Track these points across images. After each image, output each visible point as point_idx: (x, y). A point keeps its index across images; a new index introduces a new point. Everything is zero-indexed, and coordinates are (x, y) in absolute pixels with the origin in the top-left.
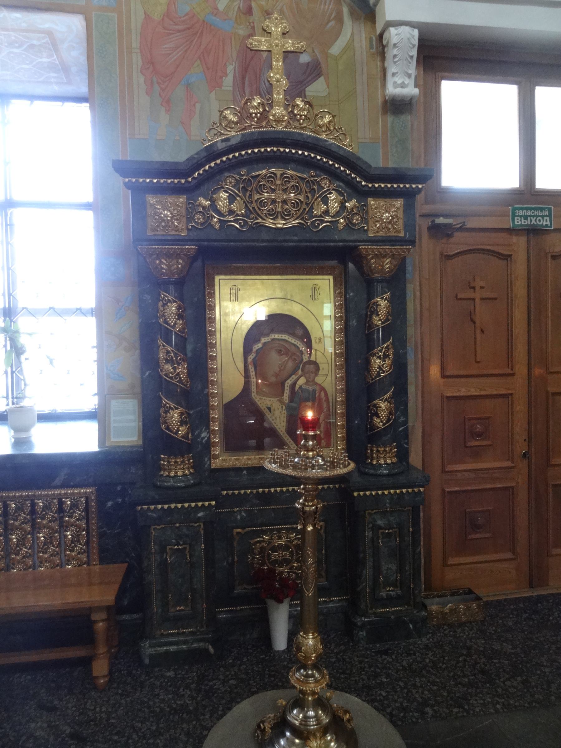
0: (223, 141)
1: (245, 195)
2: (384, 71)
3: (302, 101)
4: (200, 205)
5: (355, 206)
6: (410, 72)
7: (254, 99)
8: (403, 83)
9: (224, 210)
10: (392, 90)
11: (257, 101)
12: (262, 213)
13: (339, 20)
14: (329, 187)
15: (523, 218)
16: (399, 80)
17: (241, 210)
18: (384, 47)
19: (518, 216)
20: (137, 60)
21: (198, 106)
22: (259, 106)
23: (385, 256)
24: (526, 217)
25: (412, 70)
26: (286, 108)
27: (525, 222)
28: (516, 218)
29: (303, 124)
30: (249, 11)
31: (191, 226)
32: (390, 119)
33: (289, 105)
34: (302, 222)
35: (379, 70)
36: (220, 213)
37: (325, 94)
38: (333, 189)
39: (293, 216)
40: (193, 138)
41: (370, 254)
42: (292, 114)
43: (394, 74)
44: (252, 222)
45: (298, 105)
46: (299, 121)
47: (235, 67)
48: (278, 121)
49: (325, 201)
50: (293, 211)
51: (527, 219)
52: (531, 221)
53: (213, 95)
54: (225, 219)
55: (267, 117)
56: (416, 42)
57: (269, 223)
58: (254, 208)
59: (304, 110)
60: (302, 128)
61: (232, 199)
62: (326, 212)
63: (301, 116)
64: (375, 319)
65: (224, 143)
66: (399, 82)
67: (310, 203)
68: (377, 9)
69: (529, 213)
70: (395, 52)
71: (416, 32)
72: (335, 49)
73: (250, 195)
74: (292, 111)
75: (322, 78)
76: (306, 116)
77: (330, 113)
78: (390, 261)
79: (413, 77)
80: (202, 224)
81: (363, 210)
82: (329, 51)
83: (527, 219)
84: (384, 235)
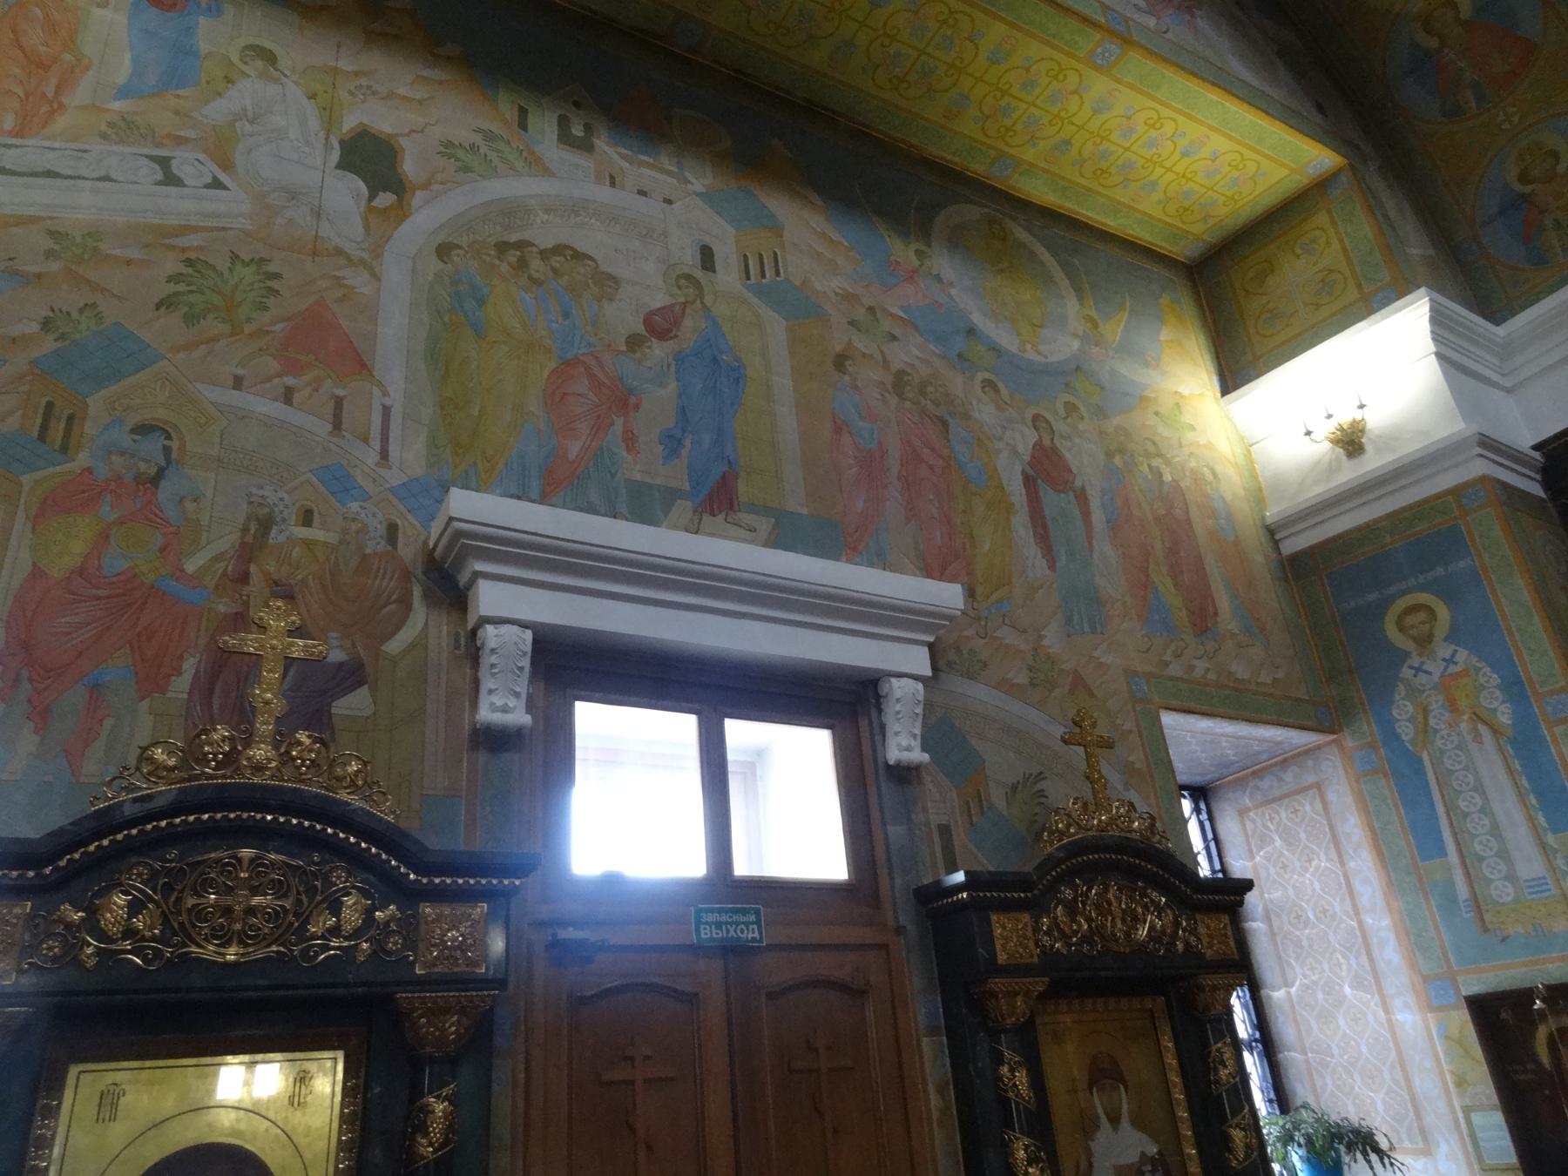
0: (135, 800)
1: (166, 897)
3: (309, 737)
4: (60, 920)
5: (392, 918)
6: (518, 689)
7: (215, 730)
9: (114, 930)
10: (485, 715)
11: (222, 731)
12: (200, 934)
13: (406, 604)
14: (345, 882)
15: (713, 927)
16: (499, 701)
17: (151, 928)
18: (478, 649)
19: (707, 923)
22: (223, 741)
23: (447, 1011)
24: (719, 925)
25: (522, 687)
26: (276, 747)
27: (717, 934)
28: (702, 927)
29: (305, 774)
30: (244, 578)
31: (28, 963)
32: (482, 757)
33: (282, 738)
34: (282, 949)
35: (468, 680)
36: (102, 936)
37: (368, 712)
38: (354, 887)
39: (264, 938)
40: (83, 780)
41: (416, 1009)
42: (286, 759)
43: (490, 692)
44: (171, 953)
45: (299, 743)
46: (298, 768)
47: (200, 662)
48: (259, 768)
49: (335, 908)
50: (267, 928)
51: (721, 930)
52: (728, 931)
53: (145, 705)
54: (114, 947)
55: (237, 760)
56: (528, 647)
57: (209, 951)
58: (181, 924)
59: (311, 751)
60: (303, 781)
61: (135, 907)
62: (335, 931)
63: (303, 761)
64: (419, 1143)
65: (138, 805)
66: (499, 703)
67: (302, 915)
68: (470, 593)
69: (724, 918)
70: (493, 659)
72: (394, 646)
73: (178, 900)
74: (288, 752)
75: (364, 691)
77: (359, 758)
78: (458, 1021)
79: (524, 696)
80: (55, 959)
81: (410, 927)
82: (383, 648)
83: (721, 930)
84: (446, 970)
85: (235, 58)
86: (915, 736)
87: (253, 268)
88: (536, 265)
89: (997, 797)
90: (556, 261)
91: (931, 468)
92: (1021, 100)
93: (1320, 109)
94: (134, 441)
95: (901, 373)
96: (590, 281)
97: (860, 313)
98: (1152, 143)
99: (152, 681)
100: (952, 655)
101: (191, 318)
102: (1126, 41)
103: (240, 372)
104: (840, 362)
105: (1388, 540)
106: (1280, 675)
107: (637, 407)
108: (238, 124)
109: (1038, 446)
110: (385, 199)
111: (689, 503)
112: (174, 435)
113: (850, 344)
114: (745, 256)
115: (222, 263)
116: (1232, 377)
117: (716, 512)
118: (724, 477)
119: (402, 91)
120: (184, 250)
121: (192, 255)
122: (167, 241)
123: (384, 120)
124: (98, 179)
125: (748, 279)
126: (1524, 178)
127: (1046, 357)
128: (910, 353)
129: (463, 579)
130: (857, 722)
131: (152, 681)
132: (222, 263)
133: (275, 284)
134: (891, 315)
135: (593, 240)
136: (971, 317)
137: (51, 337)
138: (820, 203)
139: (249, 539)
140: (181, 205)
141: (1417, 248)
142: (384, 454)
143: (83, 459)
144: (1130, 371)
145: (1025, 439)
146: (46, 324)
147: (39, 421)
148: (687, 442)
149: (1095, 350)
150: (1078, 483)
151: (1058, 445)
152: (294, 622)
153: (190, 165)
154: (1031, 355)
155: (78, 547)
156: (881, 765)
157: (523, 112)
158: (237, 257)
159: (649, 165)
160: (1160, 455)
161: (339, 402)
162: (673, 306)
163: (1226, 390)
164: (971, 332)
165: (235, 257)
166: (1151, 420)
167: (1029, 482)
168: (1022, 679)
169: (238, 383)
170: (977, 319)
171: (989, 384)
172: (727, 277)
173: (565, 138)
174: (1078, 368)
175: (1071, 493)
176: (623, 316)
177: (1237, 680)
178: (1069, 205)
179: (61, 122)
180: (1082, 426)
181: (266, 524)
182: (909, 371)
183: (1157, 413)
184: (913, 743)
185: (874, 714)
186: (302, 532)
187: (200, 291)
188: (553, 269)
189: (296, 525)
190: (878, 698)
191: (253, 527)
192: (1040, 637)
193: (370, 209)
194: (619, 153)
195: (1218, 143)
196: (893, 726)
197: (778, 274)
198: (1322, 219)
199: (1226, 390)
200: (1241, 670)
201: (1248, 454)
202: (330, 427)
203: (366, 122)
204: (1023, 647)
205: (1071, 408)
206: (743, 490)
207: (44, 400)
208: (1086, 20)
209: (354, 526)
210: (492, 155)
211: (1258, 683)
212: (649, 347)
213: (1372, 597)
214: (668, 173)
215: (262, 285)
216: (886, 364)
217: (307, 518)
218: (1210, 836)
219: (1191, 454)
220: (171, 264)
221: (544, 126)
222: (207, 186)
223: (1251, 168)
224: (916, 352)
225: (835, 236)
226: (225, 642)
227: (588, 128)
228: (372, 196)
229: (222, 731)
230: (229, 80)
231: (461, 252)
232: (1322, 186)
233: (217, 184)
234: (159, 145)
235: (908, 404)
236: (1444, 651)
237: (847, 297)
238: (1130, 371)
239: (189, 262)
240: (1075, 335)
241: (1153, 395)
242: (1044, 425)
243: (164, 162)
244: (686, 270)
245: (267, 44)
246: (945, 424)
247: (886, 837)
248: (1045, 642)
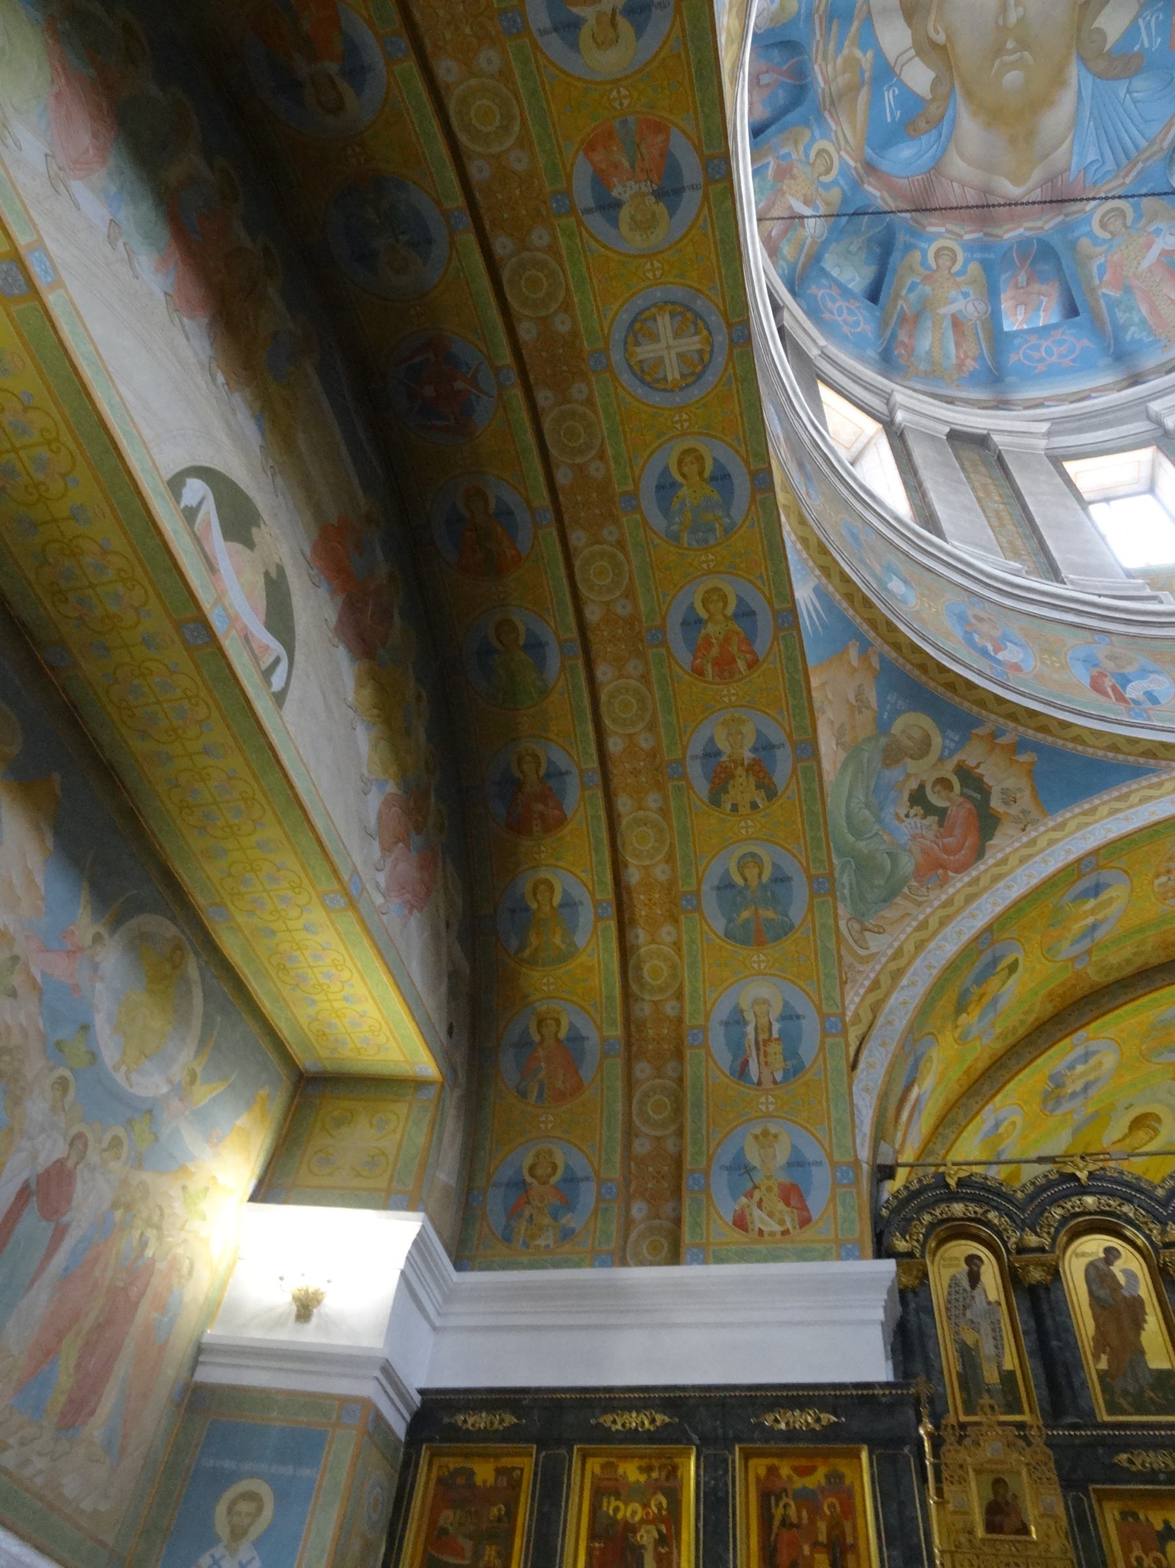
92: (262, 883)
98: (329, 976)
102: (352, 904)
105: (274, 1414)
109: (60, 1164)
126: (532, 1169)
127: (131, 1086)
138: (50, 843)
141: (446, 1174)
144: (190, 1137)
145: (52, 1149)
149: (175, 1103)
150: (65, 1219)
151: (78, 1172)
154: (120, 1078)
160: (159, 1228)
163: (253, 1198)
164: (86, 1028)
166: (175, 1192)
170: (100, 1022)
171: (63, 1084)
174: (150, 1111)
175: (53, 1225)
180: (113, 1165)
183: (184, 1188)
195: (369, 1007)
198: (402, 1108)
199: (253, 1198)
200: (70, 1487)
205: (116, 1143)
208: (335, 871)
213: (228, 1464)
219: (185, 1241)
223: (382, 1039)
225: (39, 879)
232: (419, 1084)
236: (245, 1551)
238: (190, 1137)
240: (170, 1081)
241: (193, 1169)
242: (81, 1146)
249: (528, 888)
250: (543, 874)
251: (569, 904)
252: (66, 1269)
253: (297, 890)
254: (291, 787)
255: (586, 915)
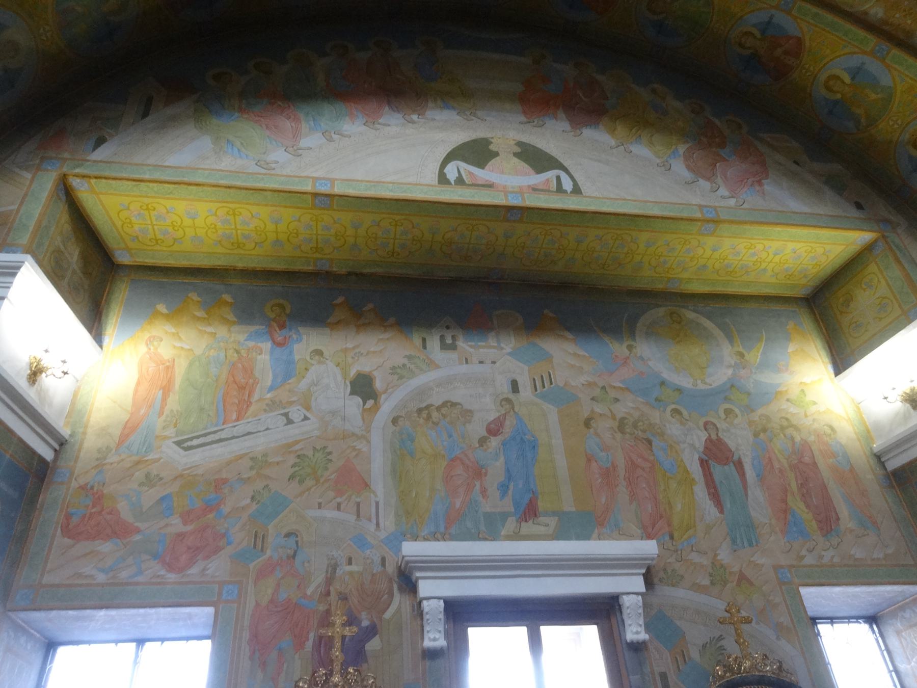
2: (422, 626)
6: (440, 629)
8: (435, 637)
10: (427, 643)
13: (391, 595)
16: (432, 636)
20: (246, 635)
21: (285, 665)
22: (323, 675)
30: (328, 594)
32: (428, 663)
45: (350, 673)
53: (297, 656)
59: (354, 675)
66: (432, 637)
71: (442, 603)
72: (388, 615)
75: (378, 636)
76: (355, 680)
85: (308, 358)
86: (641, 626)
87: (321, 451)
88: (435, 415)
89: (695, 654)
90: (444, 410)
91: (643, 469)
93: (859, 206)
94: (286, 541)
95: (622, 419)
96: (460, 416)
97: (597, 392)
98: (754, 254)
99: (299, 645)
100: (662, 574)
101: (301, 482)
102: (716, 222)
103: (320, 500)
104: (587, 423)
106: (890, 551)
107: (486, 474)
108: (311, 389)
109: (709, 440)
110: (370, 403)
111: (514, 518)
112: (299, 536)
113: (592, 411)
114: (534, 379)
115: (310, 453)
116: (841, 363)
117: (528, 520)
118: (531, 501)
119: (372, 349)
120: (296, 451)
121: (299, 453)
122: (290, 450)
123: (364, 365)
124: (264, 431)
125: (536, 390)
127: (711, 385)
128: (627, 406)
129: (414, 580)
130: (610, 620)
131: (299, 645)
132: (310, 453)
133: (329, 457)
134: (614, 387)
135: (459, 394)
136: (662, 375)
137: (254, 503)
138: (571, 336)
139: (329, 575)
140: (293, 432)
142: (378, 524)
143: (269, 553)
144: (767, 378)
145: (699, 438)
146: (253, 498)
147: (253, 540)
148: (511, 487)
149: (742, 372)
150: (736, 458)
151: (721, 437)
152: (344, 620)
153: (296, 413)
154: (701, 386)
155: (270, 591)
156: (624, 642)
157: (424, 340)
158: (315, 448)
159: (483, 347)
161: (358, 504)
162: (499, 417)
163: (838, 371)
164: (663, 383)
165: (314, 448)
166: (784, 406)
167: (704, 463)
168: (706, 582)
169: (320, 506)
170: (666, 375)
171: (676, 411)
172: (526, 392)
173: (444, 347)
174: (732, 386)
175: (732, 464)
176: (477, 429)
177: (856, 560)
178: (719, 289)
179: (252, 409)
181: (334, 567)
182: (628, 417)
183: (788, 400)
184: (639, 629)
185: (618, 614)
186: (348, 568)
187: (303, 468)
188: (442, 414)
189: (346, 565)
190: (620, 606)
191: (330, 569)
192: (716, 555)
193: (364, 410)
194: (469, 346)
195: (791, 246)
196: (628, 622)
197: (551, 383)
198: (873, 268)
199: (838, 371)
200: (858, 553)
201: (858, 410)
202: (355, 517)
203: (359, 369)
204: (705, 563)
205: (728, 412)
206: (541, 505)
207: (255, 530)
208: (691, 220)
209: (368, 561)
210: (412, 367)
211: (873, 560)
212: (490, 442)
214: (494, 347)
215: (326, 459)
216: (614, 417)
217: (350, 562)
218: (883, 648)
219: (814, 420)
220: (292, 459)
221: (434, 343)
222: (303, 420)
223: (820, 250)
224: (631, 405)
225: (581, 353)
226: (321, 633)
227: (453, 337)
228: (364, 404)
229: (322, 671)
230: (307, 369)
231: (402, 419)
232: (869, 249)
233: (306, 418)
234: (284, 408)
235: (628, 436)
237: (590, 385)
238: (767, 378)
239: (298, 457)
240: (729, 366)
241: (785, 389)
243: (286, 415)
244: (505, 396)
245: (320, 348)
246: (650, 442)
247: (630, 682)
248: (719, 558)
249: (823, 92)
250: (823, 77)
251: (855, 73)
252: (758, 476)
253: (687, 243)
254: (624, 215)
255: (873, 66)
